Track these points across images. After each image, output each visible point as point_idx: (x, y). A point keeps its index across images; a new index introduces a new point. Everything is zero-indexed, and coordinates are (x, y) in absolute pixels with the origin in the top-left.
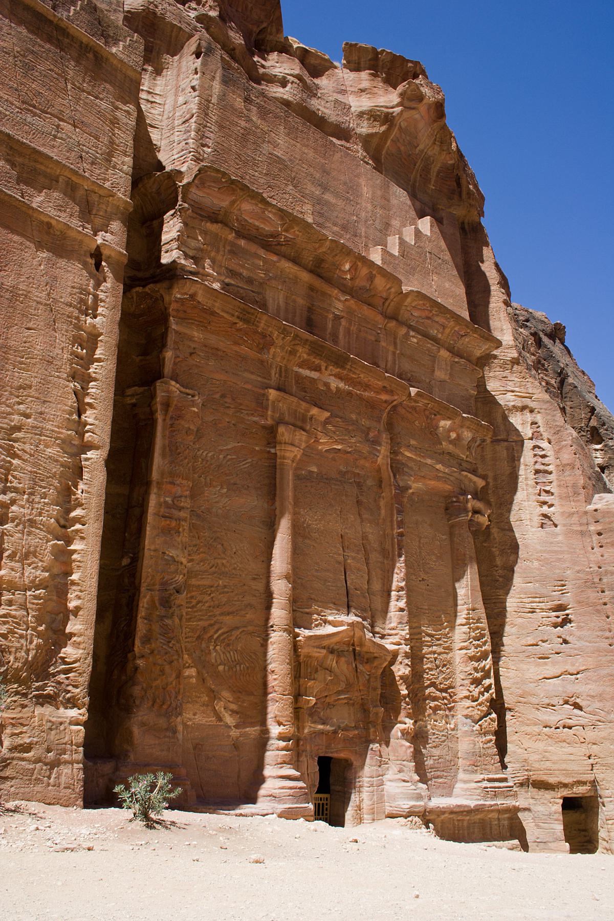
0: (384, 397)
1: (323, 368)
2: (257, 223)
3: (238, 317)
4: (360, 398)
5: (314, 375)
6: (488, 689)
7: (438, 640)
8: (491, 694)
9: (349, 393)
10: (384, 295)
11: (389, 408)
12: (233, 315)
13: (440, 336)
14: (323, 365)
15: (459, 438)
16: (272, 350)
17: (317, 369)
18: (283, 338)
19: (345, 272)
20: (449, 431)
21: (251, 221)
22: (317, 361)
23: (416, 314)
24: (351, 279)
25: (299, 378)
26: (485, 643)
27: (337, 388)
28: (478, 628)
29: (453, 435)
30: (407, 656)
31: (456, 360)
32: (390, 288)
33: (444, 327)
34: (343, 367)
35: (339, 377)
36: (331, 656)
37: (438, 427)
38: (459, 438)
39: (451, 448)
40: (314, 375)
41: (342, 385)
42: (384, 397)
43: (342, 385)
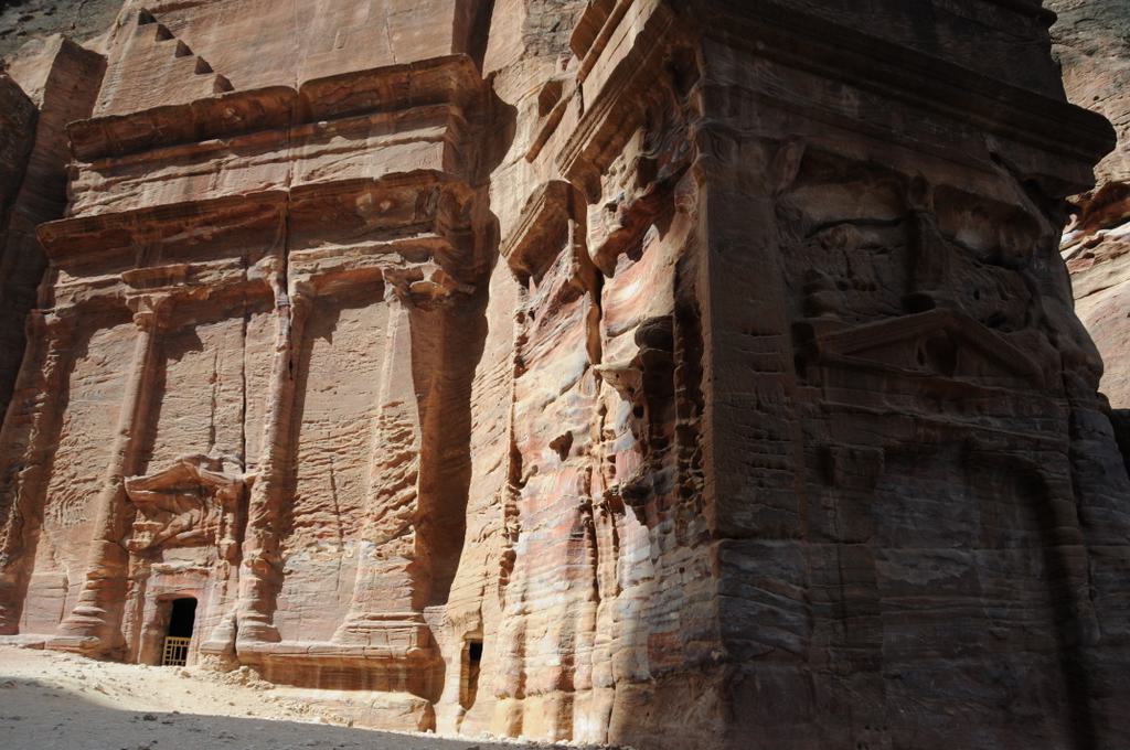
0: (269, 214)
1: (184, 226)
2: (137, 136)
3: (86, 231)
4: (244, 229)
5: (183, 236)
6: (406, 501)
7: (344, 453)
8: (411, 508)
9: (229, 232)
10: (285, 108)
11: (283, 221)
12: (81, 232)
13: (378, 102)
14: (182, 222)
15: (396, 204)
16: (135, 237)
17: (181, 230)
18: (130, 225)
19: (231, 118)
20: (377, 202)
21: (131, 138)
22: (175, 223)
23: (332, 101)
24: (243, 118)
25: (166, 247)
26: (410, 442)
27: (213, 234)
28: (398, 426)
29: (386, 205)
30: (264, 479)
31: (401, 115)
32: (282, 100)
33: (376, 91)
34: (197, 215)
35: (208, 223)
36: (167, 497)
37: (355, 208)
38: (396, 204)
39: (382, 221)
40: (183, 236)
41: (215, 229)
42: (269, 214)
43: (215, 229)
